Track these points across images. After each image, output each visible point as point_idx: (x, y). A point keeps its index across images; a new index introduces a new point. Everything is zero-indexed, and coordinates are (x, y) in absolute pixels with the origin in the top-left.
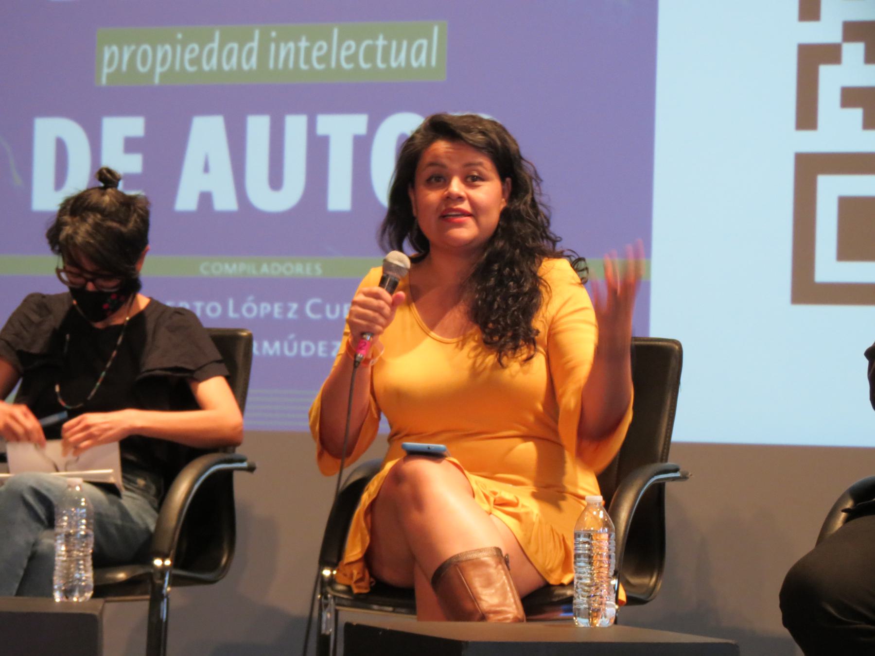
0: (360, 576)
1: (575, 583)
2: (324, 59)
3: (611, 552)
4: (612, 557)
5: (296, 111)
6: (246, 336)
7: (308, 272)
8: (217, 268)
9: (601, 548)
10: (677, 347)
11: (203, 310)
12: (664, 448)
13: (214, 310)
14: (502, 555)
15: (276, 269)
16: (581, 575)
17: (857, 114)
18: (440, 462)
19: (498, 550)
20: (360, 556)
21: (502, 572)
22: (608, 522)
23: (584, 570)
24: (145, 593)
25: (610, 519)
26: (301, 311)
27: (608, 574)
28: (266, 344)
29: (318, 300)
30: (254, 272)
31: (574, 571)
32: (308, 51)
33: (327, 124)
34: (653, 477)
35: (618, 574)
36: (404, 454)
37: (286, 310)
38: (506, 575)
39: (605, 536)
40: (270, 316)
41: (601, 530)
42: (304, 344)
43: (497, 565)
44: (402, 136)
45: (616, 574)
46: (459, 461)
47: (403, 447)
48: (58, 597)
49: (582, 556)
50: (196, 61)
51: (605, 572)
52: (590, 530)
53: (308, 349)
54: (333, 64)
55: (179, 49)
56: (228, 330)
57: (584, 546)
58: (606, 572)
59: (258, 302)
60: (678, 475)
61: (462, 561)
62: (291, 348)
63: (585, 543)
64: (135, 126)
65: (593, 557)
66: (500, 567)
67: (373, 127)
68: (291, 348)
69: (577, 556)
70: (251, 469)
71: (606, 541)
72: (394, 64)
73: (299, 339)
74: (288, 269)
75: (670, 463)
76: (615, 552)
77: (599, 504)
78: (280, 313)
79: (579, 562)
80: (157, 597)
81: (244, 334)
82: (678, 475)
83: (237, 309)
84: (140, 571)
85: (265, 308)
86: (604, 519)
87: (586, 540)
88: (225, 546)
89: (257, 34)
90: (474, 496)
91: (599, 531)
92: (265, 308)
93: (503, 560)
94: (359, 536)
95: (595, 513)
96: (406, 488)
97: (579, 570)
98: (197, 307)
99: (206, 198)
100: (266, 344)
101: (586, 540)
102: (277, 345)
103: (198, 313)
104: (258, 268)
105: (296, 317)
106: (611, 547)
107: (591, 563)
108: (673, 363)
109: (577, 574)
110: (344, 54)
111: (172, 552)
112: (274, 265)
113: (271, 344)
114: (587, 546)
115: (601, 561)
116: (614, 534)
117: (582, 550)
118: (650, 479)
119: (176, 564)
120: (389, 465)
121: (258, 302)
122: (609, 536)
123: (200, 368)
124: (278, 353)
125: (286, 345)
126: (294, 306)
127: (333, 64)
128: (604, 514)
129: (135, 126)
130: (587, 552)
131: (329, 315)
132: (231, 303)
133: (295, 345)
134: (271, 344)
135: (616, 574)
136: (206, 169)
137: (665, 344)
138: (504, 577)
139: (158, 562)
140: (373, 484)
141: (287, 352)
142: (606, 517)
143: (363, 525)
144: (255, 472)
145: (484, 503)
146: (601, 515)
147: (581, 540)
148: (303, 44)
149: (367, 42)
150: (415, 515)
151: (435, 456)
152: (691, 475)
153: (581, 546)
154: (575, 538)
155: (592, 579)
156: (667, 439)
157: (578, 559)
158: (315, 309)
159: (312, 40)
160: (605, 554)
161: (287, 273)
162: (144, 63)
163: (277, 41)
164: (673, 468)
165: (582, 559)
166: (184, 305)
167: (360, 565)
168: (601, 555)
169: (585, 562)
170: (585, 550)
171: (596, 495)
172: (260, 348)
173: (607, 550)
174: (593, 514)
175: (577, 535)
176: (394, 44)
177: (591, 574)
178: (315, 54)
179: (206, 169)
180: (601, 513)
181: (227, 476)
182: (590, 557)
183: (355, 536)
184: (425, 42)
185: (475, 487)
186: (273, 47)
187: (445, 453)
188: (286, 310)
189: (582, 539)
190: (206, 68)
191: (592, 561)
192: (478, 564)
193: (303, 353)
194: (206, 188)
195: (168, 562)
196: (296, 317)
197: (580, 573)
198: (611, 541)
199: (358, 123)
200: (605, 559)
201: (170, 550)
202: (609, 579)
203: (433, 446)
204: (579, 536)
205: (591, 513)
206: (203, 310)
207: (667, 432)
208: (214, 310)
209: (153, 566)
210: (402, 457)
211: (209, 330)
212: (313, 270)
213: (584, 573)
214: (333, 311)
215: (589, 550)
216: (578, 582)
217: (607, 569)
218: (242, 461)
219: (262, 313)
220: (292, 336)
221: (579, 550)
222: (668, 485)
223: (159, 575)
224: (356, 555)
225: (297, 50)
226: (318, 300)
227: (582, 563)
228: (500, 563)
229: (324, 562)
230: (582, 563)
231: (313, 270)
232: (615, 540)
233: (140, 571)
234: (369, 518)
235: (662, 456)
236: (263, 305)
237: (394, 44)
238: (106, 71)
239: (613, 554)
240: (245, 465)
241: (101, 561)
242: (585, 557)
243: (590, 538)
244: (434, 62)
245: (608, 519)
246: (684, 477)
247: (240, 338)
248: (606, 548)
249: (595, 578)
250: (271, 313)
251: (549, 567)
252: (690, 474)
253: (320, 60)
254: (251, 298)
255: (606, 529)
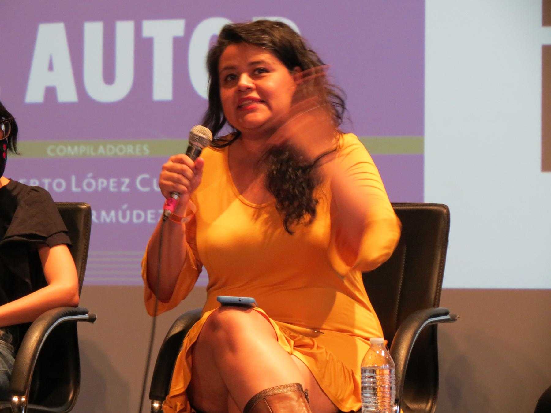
0: (183, 407)
1: (362, 411)
3: (392, 384)
4: (393, 388)
5: (125, 17)
6: (85, 208)
7: (138, 153)
8: (61, 151)
9: (383, 381)
10: (445, 211)
12: (436, 296)
13: (59, 185)
14: (302, 391)
15: (111, 150)
16: (367, 404)
18: (249, 312)
19: (299, 386)
20: (183, 390)
21: (303, 404)
22: (389, 360)
23: (370, 400)
25: (390, 357)
26: (132, 185)
27: (390, 403)
28: (103, 213)
29: (147, 176)
30: (93, 154)
31: (362, 401)
34: (427, 320)
35: (399, 402)
36: (219, 305)
37: (119, 184)
38: (306, 406)
39: (387, 372)
40: (106, 189)
41: (383, 366)
42: (135, 212)
43: (299, 398)
44: (213, 37)
45: (397, 402)
46: (264, 310)
47: (218, 300)
49: (368, 388)
51: (387, 401)
52: (375, 367)
53: (139, 216)
56: (71, 204)
57: (369, 380)
58: (388, 401)
59: (95, 178)
60: (448, 317)
61: (269, 396)
62: (124, 217)
63: (370, 377)
65: (376, 389)
66: (301, 400)
67: (189, 30)
68: (124, 217)
69: (364, 388)
70: (92, 320)
71: (388, 376)
73: (131, 208)
74: (121, 150)
75: (441, 308)
76: (396, 385)
77: (381, 345)
78: (114, 187)
79: (365, 393)
81: (84, 207)
82: (448, 317)
83: (79, 185)
85: (102, 183)
86: (386, 357)
87: (371, 374)
90: (278, 340)
91: (381, 367)
92: (102, 183)
93: (303, 395)
94: (182, 374)
95: (378, 352)
96: (221, 334)
97: (366, 400)
98: (46, 184)
99: (51, 92)
100: (103, 213)
101: (371, 374)
102: (113, 213)
103: (46, 188)
104: (96, 150)
105: (128, 190)
106: (392, 381)
107: (375, 394)
108: (443, 223)
109: (364, 403)
112: (108, 147)
113: (108, 214)
114: (372, 380)
115: (383, 392)
116: (395, 369)
117: (368, 383)
118: (425, 321)
119: (30, 400)
120: (206, 315)
122: (390, 372)
123: (51, 236)
124: (114, 220)
125: (120, 213)
126: (127, 181)
128: (385, 353)
130: (372, 385)
132: (74, 178)
133: (128, 213)
134: (108, 214)
135: (397, 402)
136: (51, 68)
137: (435, 208)
138: (305, 408)
139: (15, 399)
140: (193, 331)
141: (121, 220)
142: (387, 355)
143: (185, 363)
144: (95, 322)
145: (286, 345)
146: (383, 354)
147: (367, 375)
150: (229, 356)
151: (244, 307)
152: (459, 317)
153: (367, 380)
154: (362, 373)
155: (377, 407)
156: (439, 287)
157: (364, 391)
158: (144, 183)
160: (387, 386)
161: (120, 154)
164: (445, 312)
165: (368, 390)
166: (34, 183)
167: (182, 398)
168: (384, 387)
169: (370, 394)
170: (371, 383)
171: (380, 337)
172: (98, 217)
173: (389, 383)
174: (376, 353)
175: (363, 371)
177: (375, 403)
179: (51, 68)
180: (383, 352)
181: (73, 324)
182: (374, 389)
183: (179, 373)
185: (279, 332)
187: (253, 305)
188: (119, 184)
189: (367, 374)
191: (377, 393)
192: (283, 398)
193: (135, 220)
194: (50, 84)
196: (128, 190)
197: (366, 402)
198: (391, 376)
200: (387, 390)
201: (25, 389)
202: (391, 407)
203: (244, 299)
204: (365, 372)
205: (375, 352)
206: (50, 185)
207: (438, 282)
208: (59, 185)
210: (218, 308)
211: (57, 204)
212: (142, 150)
213: (370, 402)
215: (374, 383)
216: (365, 410)
217: (389, 399)
218: (84, 313)
219: (100, 189)
220: (125, 206)
221: (365, 383)
223: (16, 410)
224: (179, 389)
226: (147, 176)
227: (368, 394)
228: (301, 396)
229: (153, 397)
230: (368, 394)
231: (142, 150)
232: (395, 375)
234: (190, 358)
235: (435, 301)
236: (100, 181)
239: (394, 387)
240: (86, 316)
242: (370, 389)
243: (375, 373)
245: (389, 357)
246: (453, 319)
247: (81, 210)
248: (388, 381)
249: (379, 407)
250: (107, 188)
251: (340, 398)
252: (458, 316)
254: (90, 175)
255: (388, 366)
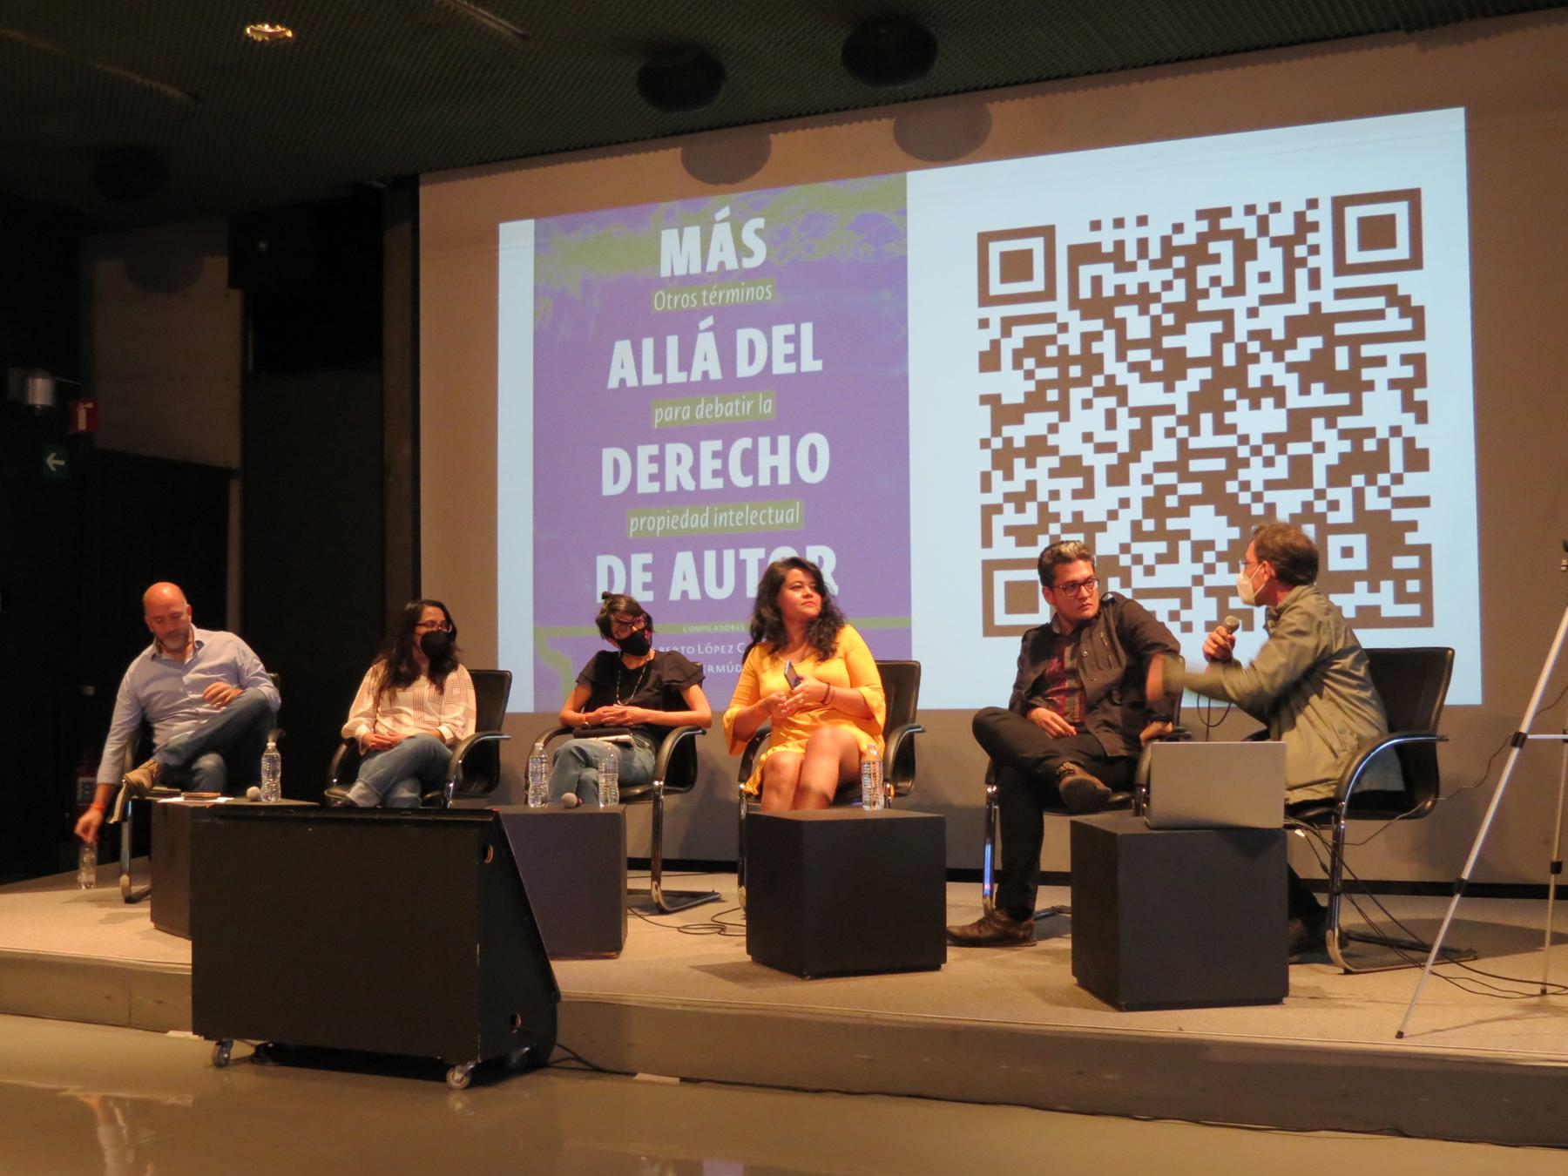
2: (742, 520)
11: (685, 651)
13: (691, 650)
17: (1012, 539)
32: (734, 517)
33: (745, 554)
37: (727, 649)
48: (602, 805)
50: (678, 524)
54: (747, 523)
59: (712, 645)
62: (730, 669)
64: (647, 558)
68: (730, 669)
72: (777, 522)
80: (657, 801)
83: (702, 649)
85: (717, 648)
99: (685, 594)
102: (723, 667)
103: (683, 653)
104: (712, 628)
108: (916, 673)
111: (664, 778)
112: (720, 626)
121: (712, 645)
127: (747, 523)
129: (647, 558)
132: (699, 646)
139: (656, 783)
148: (731, 513)
149: (764, 511)
163: (718, 512)
176: (777, 512)
184: (793, 510)
190: (682, 527)
206: (685, 651)
208: (691, 650)
209: (654, 785)
212: (740, 628)
219: (715, 651)
225: (728, 516)
231: (740, 628)
236: (715, 647)
237: (777, 512)
238: (632, 530)
241: (623, 784)
246: (923, 731)
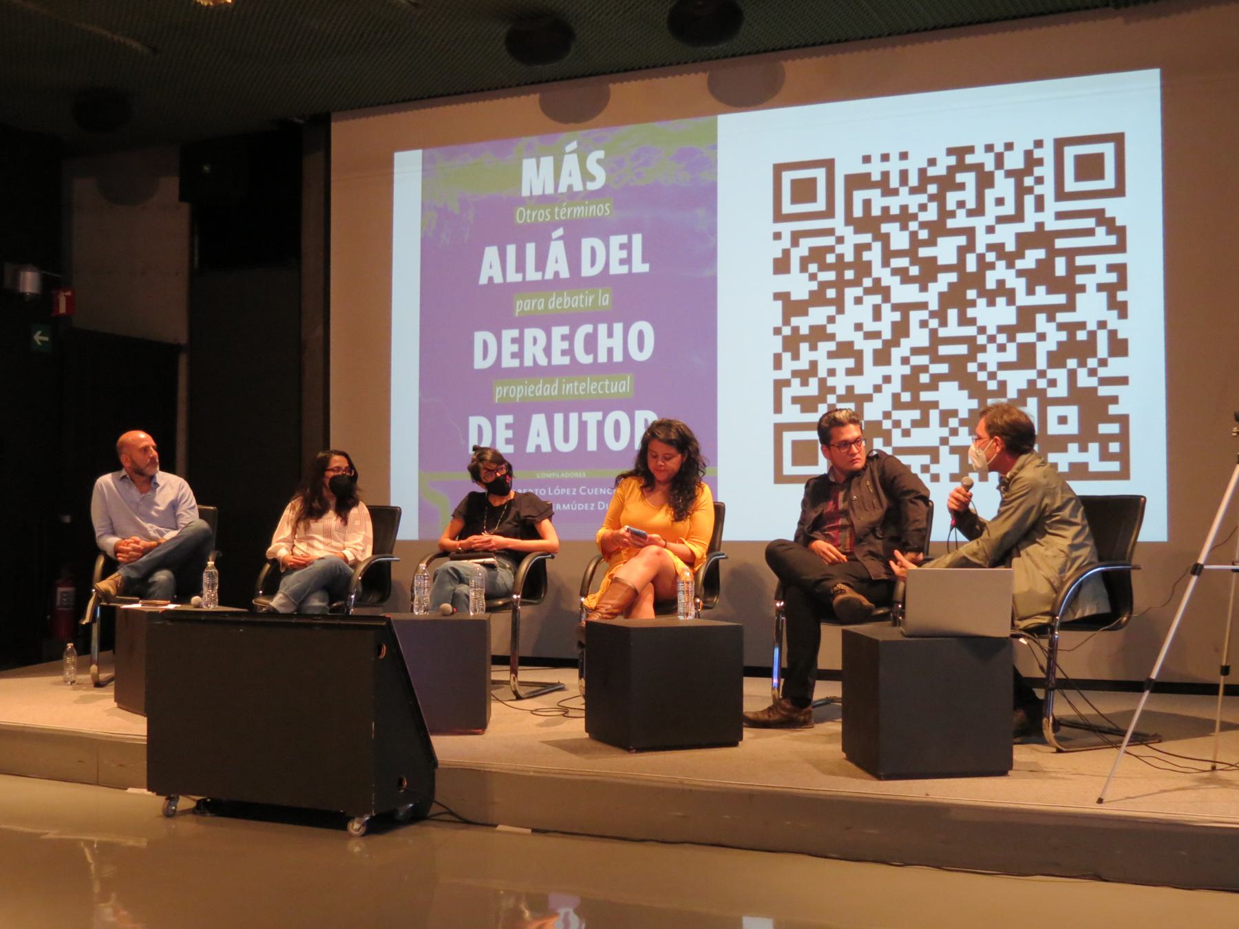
2: (584, 390)
7: (580, 476)
11: (538, 492)
13: (543, 492)
24: (510, 609)
26: (577, 491)
29: (584, 487)
33: (587, 416)
48: (472, 614)
50: (533, 392)
53: (581, 507)
54: (588, 392)
55: (526, 387)
60: (724, 556)
62: (574, 507)
64: (509, 419)
67: (604, 417)
68: (574, 507)
72: (612, 391)
73: (577, 503)
75: (721, 552)
80: (515, 611)
82: (724, 556)
83: (552, 492)
84: (507, 600)
85: (563, 491)
88: (543, 589)
89: (557, 380)
99: (538, 447)
100: (564, 505)
102: (568, 505)
103: (536, 494)
110: (592, 388)
113: (566, 505)
129: (509, 419)
131: (589, 493)
139: (515, 597)
158: (584, 490)
159: (579, 382)
162: (512, 394)
176: (612, 383)
178: (581, 388)
184: (624, 382)
186: (564, 385)
190: (537, 395)
193: (579, 509)
195: (519, 596)
199: (598, 415)
206: (538, 492)
208: (543, 492)
212: (582, 475)
214: (591, 492)
222: (721, 561)
225: (574, 386)
226: (584, 487)
231: (582, 475)
233: (507, 600)
237: (612, 383)
238: (497, 397)
244: (628, 390)
246: (726, 558)
253: (583, 390)
254: (558, 487)
